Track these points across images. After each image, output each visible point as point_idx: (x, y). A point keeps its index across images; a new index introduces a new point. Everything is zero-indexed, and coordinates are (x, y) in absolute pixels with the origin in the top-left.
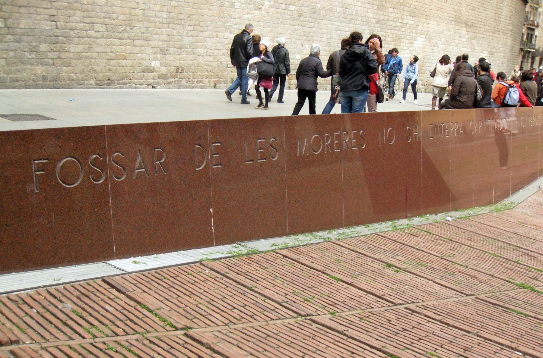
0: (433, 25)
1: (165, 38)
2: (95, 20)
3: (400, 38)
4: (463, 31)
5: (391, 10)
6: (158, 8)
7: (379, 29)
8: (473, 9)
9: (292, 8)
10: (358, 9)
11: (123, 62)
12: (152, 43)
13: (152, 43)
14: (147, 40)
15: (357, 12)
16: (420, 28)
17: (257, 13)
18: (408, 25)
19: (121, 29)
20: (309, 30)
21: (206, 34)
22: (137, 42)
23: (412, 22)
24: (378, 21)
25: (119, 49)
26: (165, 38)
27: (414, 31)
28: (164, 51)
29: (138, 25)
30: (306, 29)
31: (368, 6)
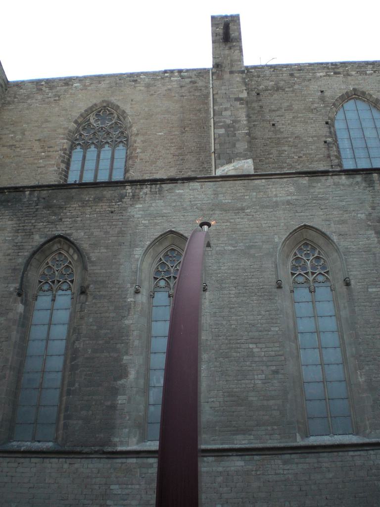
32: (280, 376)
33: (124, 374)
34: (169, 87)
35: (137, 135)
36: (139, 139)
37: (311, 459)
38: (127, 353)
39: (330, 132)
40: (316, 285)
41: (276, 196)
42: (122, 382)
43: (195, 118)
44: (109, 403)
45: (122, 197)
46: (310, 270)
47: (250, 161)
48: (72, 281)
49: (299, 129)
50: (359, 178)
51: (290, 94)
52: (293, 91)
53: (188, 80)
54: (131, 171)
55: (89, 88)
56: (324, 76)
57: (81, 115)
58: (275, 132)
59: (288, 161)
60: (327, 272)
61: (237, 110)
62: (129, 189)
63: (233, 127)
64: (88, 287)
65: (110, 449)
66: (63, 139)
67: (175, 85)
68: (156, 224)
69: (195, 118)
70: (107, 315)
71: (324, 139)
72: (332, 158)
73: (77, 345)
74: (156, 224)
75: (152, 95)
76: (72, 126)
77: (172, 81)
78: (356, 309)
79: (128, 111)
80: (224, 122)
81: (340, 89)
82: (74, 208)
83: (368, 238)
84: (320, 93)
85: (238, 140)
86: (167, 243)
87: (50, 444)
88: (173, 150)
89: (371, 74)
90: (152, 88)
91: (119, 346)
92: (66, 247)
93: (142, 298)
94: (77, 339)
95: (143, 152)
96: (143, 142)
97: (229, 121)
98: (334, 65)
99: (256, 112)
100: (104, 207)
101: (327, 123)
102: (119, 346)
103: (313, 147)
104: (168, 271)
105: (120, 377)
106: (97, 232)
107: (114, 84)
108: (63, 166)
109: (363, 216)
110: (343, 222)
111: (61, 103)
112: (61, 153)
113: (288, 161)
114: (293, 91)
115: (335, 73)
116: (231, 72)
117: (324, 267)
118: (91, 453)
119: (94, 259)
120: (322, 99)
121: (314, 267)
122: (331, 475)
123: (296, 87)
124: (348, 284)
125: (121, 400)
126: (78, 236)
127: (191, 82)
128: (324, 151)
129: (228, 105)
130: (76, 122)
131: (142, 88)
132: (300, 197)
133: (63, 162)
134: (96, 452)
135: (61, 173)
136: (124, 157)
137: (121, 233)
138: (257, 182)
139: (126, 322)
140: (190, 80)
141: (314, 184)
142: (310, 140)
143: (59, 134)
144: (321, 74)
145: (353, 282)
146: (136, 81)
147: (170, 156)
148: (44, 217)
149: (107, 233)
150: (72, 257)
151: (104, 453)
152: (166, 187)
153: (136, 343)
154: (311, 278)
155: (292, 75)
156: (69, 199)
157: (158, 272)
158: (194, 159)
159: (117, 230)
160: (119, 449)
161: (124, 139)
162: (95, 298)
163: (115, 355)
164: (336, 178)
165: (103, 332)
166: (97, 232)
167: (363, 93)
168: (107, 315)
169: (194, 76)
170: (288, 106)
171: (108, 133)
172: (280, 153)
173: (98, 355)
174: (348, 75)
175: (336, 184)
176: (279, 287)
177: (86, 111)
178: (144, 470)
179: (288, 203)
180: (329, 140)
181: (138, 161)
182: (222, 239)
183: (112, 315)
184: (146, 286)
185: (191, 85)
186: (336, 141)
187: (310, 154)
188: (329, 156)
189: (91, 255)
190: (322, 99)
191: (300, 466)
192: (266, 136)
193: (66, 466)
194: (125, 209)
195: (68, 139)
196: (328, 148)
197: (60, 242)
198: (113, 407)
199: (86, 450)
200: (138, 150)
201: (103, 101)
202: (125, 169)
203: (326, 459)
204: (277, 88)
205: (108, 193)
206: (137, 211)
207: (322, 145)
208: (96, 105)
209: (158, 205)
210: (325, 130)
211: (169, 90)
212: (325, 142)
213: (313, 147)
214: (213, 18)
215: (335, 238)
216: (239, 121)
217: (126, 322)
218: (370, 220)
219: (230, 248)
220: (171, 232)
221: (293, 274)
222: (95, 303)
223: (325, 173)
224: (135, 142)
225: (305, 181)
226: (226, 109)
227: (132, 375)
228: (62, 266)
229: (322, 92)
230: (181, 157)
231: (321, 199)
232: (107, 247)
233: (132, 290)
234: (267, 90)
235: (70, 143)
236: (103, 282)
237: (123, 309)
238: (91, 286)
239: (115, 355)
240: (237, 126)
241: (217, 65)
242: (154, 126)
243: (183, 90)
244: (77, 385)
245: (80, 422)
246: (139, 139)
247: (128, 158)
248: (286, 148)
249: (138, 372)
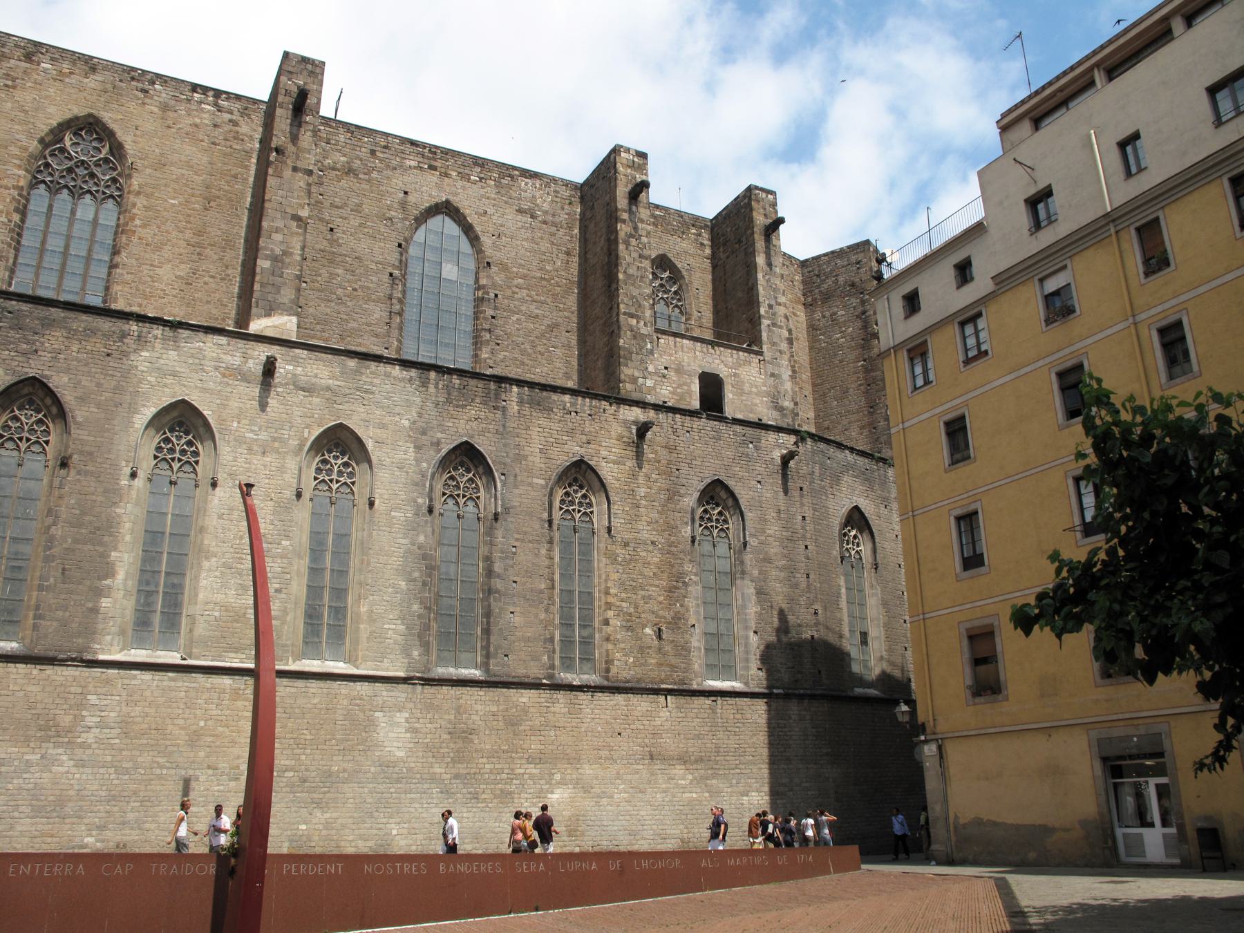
0: (588, 771)
1: (104, 815)
2: (20, 803)
3: (511, 793)
4: (679, 770)
5: (484, 760)
6: (95, 787)
7: (461, 786)
8: (698, 737)
9: (291, 774)
10: (413, 765)
11: (49, 840)
12: (86, 821)
13: (86, 821)
14: (79, 817)
15: (410, 770)
16: (558, 777)
17: (233, 784)
18: (526, 776)
19: (49, 809)
20: (321, 796)
21: (157, 809)
22: (67, 821)
23: (534, 771)
24: (457, 776)
25: (46, 827)
26: (104, 815)
27: (542, 782)
28: (101, 828)
29: (70, 804)
30: (315, 796)
31: (431, 760)
32: (283, 596)
33: (110, 573)
34: (197, 121)
35: (138, 193)
36: (141, 202)
37: (300, 683)
38: (115, 550)
39: (401, 261)
40: (338, 495)
41: (316, 376)
42: (108, 582)
43: (226, 188)
44: (90, 605)
45: (124, 335)
46: (335, 477)
47: (294, 319)
48: (47, 442)
49: (363, 247)
50: (413, 373)
51: (364, 186)
52: (369, 181)
53: (227, 116)
54: (123, 254)
55: (67, 80)
56: (415, 168)
57: (52, 131)
58: (333, 242)
59: (339, 292)
60: (353, 483)
61: (292, 234)
62: (134, 327)
63: (282, 262)
64: (70, 457)
65: (89, 657)
66: (19, 167)
67: (206, 119)
68: (166, 386)
69: (226, 188)
70: (94, 497)
71: (390, 270)
72: (394, 301)
73: (53, 530)
74: (166, 386)
75: (168, 127)
76: (34, 146)
77: (202, 110)
78: (375, 533)
79: (129, 147)
80: (272, 250)
81: (430, 195)
82: (54, 339)
83: (405, 453)
84: (402, 195)
85: (285, 284)
86: (175, 414)
87: (14, 645)
88: (188, 235)
89: (475, 183)
90: (171, 114)
91: (106, 539)
92: (41, 393)
93: (139, 482)
94: (55, 524)
95: (144, 226)
96: (147, 208)
97: (278, 252)
98: (434, 150)
99: (313, 201)
100: (96, 344)
101: (400, 245)
102: (106, 539)
103: (374, 279)
104: (172, 450)
105: (106, 577)
106: (85, 381)
107: (109, 87)
108: (16, 217)
109: (407, 423)
110: (382, 426)
111: (18, 95)
112: (15, 193)
113: (339, 292)
114: (369, 181)
115: (431, 167)
116: (295, 169)
117: (351, 475)
118: (67, 660)
119: (79, 419)
120: (403, 205)
121: (340, 473)
122: (315, 701)
123: (375, 175)
124: (372, 504)
125: (105, 602)
126: (59, 382)
127: (230, 121)
128: (385, 288)
129: (280, 224)
130: (41, 141)
131: (156, 110)
132: (342, 384)
133: (17, 210)
134: (73, 660)
135: (12, 231)
136: (114, 224)
137: (119, 389)
138: (297, 351)
139: (118, 511)
140: (229, 116)
141: (363, 370)
142: (373, 266)
143: (13, 156)
144: (413, 163)
145: (377, 502)
146: (146, 91)
147: (182, 244)
148: (11, 343)
149: (99, 385)
150: (48, 408)
151: (82, 661)
152: (184, 333)
153: (128, 538)
154: (334, 486)
155: (373, 152)
156: (48, 324)
157: (159, 449)
158: (216, 257)
159: (114, 383)
160: (101, 657)
161: (116, 193)
162: (79, 473)
163: (101, 549)
164: (389, 368)
165: (87, 518)
166: (85, 381)
167: (457, 210)
168: (94, 497)
169: (236, 112)
170: (357, 205)
171: (92, 175)
172: (332, 276)
173: (80, 546)
174: (447, 175)
175: (388, 375)
176: (299, 495)
177: (60, 125)
178: (126, 682)
179: (328, 388)
180: (397, 273)
181: (135, 240)
182: (243, 422)
183: (100, 499)
184: (146, 465)
185: (230, 127)
186: (404, 276)
187: (368, 288)
188: (390, 298)
189: (77, 412)
190: (403, 205)
191: (288, 689)
192: (318, 246)
193: (35, 672)
194: (126, 354)
195: (27, 171)
196: (393, 285)
197: (33, 385)
198: (95, 610)
199: (62, 656)
200: (137, 222)
201: (91, 115)
202: (114, 246)
203: (313, 685)
204: (349, 171)
205: (105, 324)
206: (142, 360)
207: (386, 278)
208: (77, 118)
209: (171, 358)
210: (394, 257)
211: (196, 126)
212: (391, 275)
213: (374, 279)
214: (286, 55)
215: (370, 445)
216: (292, 254)
217: (118, 511)
218: (412, 429)
219: (251, 435)
220: (183, 401)
221: (316, 479)
222: (79, 481)
223: (378, 358)
224: (134, 205)
225: (352, 363)
226: (277, 230)
227: (120, 576)
228: (34, 419)
229: (406, 193)
230: (198, 250)
231: (366, 391)
232: (98, 406)
233: (128, 471)
234: (334, 169)
235: (29, 177)
236: (91, 454)
237: (114, 495)
238: (75, 456)
239: (101, 549)
240: (287, 261)
241: (297, 314)
242: (166, 186)
243: (217, 132)
244: (52, 580)
245: (55, 624)
246: (141, 202)
247: (119, 230)
248: (340, 271)
249: (127, 573)
